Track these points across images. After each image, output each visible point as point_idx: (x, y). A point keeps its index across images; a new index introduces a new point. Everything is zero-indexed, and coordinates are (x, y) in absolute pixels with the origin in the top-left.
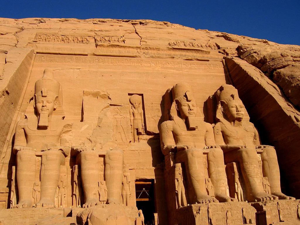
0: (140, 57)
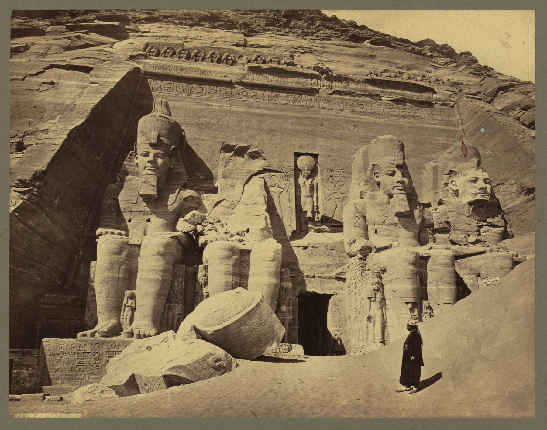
0: (317, 91)
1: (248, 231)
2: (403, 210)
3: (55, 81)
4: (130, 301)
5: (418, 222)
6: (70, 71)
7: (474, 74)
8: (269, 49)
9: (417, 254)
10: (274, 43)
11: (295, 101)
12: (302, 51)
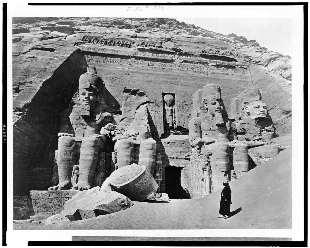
0: (174, 61)
1: (138, 134)
2: (220, 123)
3: (35, 56)
4: (76, 171)
5: (228, 129)
6: (43, 51)
7: (257, 52)
8: (149, 39)
9: (228, 146)
10: (151, 36)
11: (162, 66)
12: (167, 40)
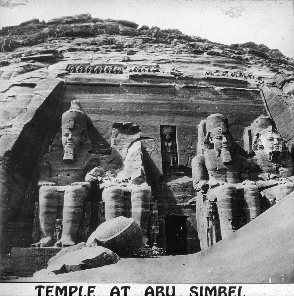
3: (15, 94)
8: (143, 62)
10: (146, 58)
12: (164, 62)
